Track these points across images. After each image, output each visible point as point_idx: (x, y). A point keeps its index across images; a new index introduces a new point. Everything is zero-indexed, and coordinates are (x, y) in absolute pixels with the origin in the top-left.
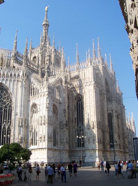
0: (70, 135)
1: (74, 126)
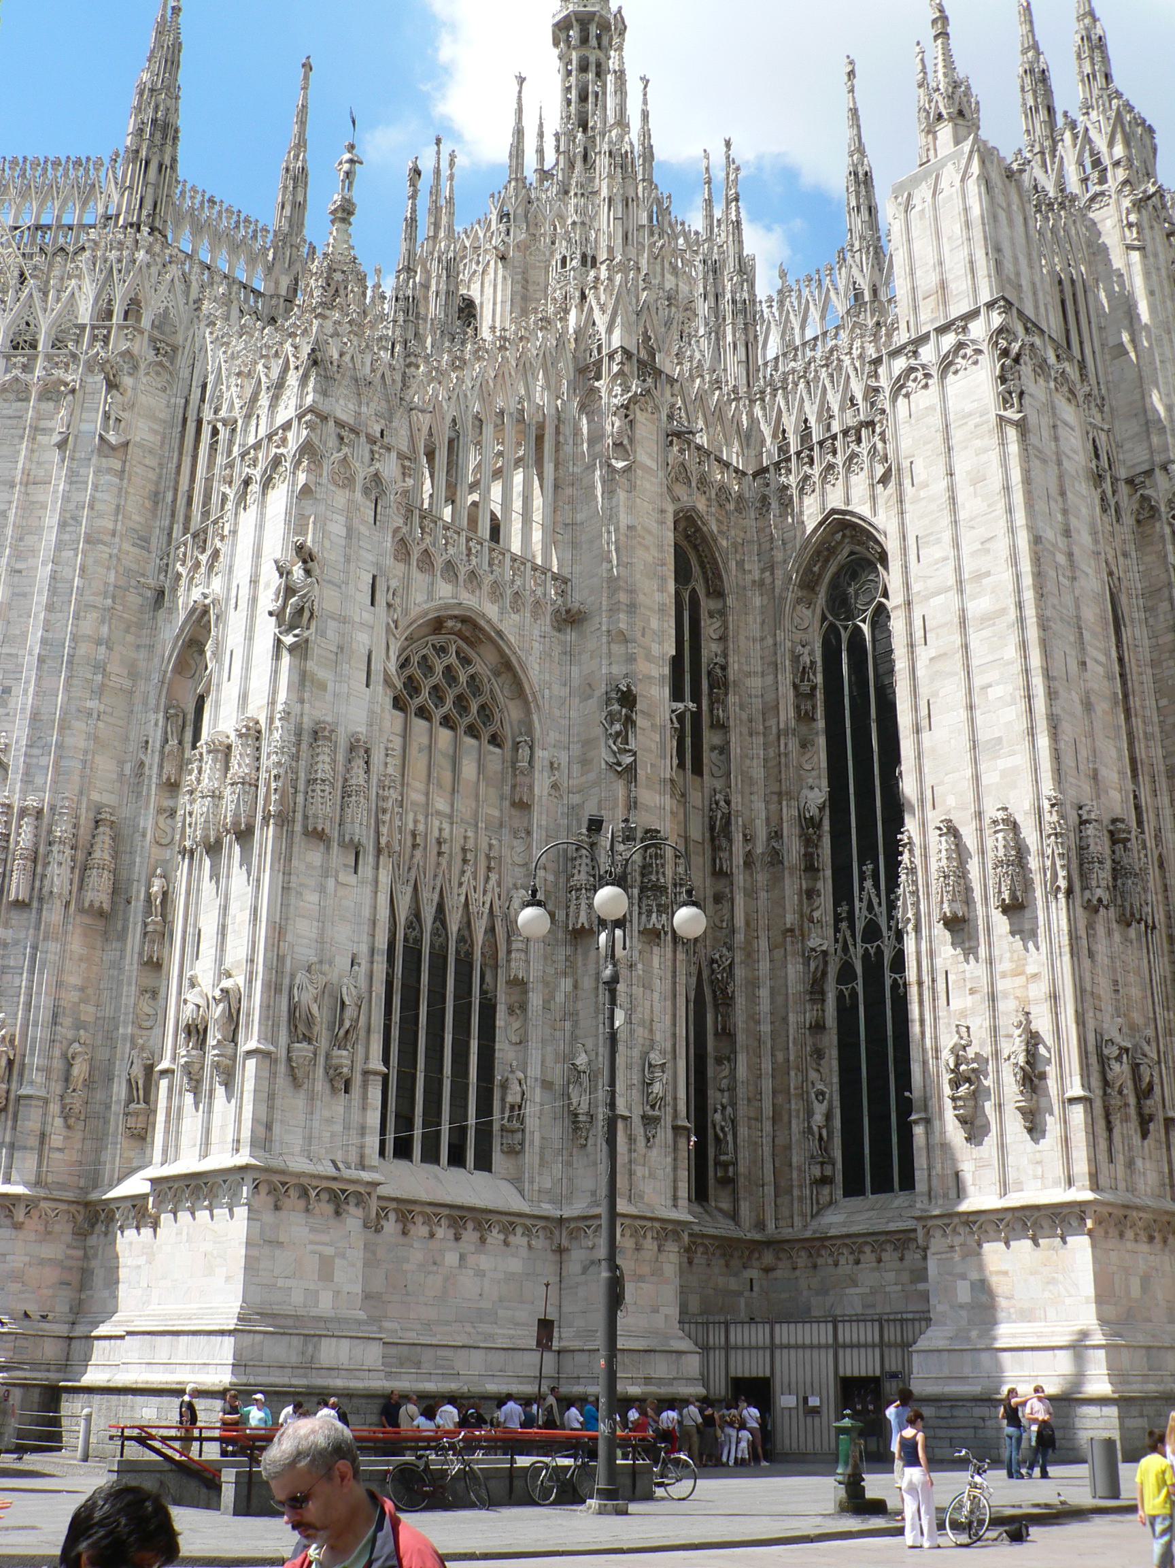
0: (741, 1038)
1: (790, 919)
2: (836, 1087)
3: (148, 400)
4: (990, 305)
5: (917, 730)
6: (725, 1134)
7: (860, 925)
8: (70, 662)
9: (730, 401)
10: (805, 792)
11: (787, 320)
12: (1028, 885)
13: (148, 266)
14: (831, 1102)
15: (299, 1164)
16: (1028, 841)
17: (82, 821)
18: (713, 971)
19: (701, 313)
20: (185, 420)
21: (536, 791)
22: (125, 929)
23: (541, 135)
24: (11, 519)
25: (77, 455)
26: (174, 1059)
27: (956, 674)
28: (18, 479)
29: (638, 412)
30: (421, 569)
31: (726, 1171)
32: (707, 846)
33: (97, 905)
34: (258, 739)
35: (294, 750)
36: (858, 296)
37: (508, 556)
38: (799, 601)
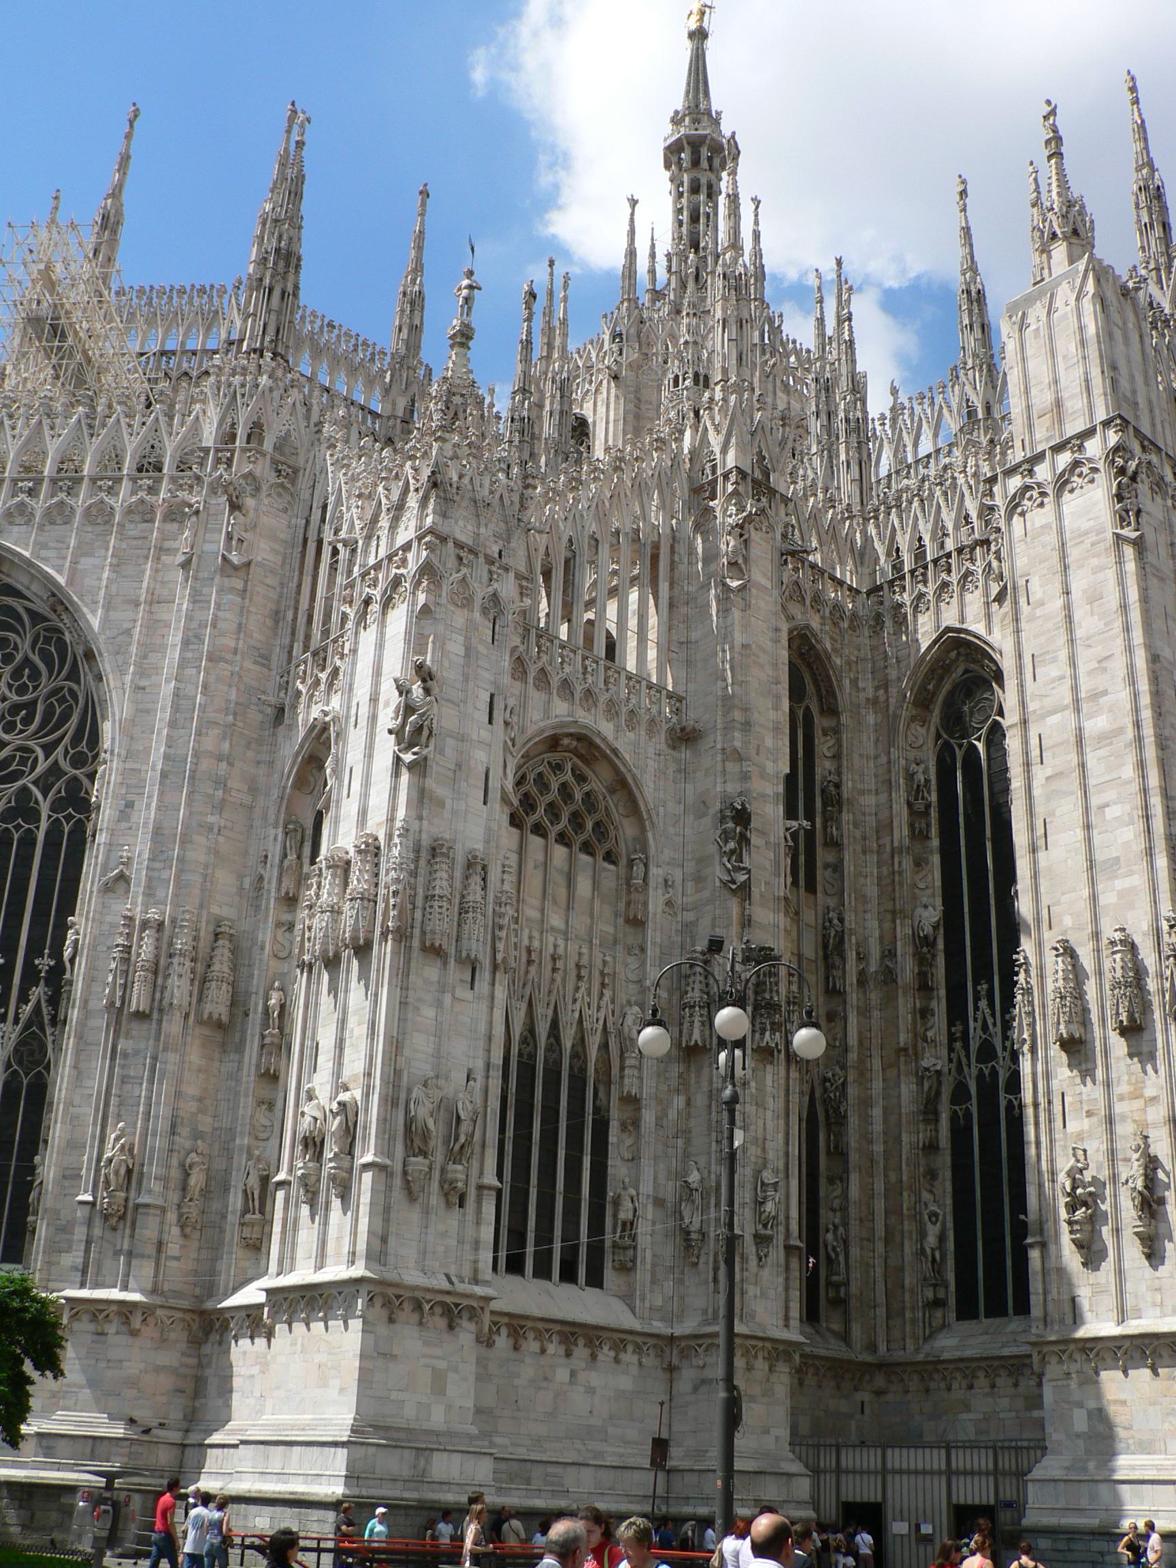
0: (854, 1157)
1: (904, 1038)
2: (949, 1209)
3: (270, 520)
4: (1106, 424)
5: (1034, 850)
6: (837, 1255)
7: (974, 1046)
8: (192, 778)
9: (844, 520)
10: (919, 910)
11: (900, 437)
12: (1146, 1007)
13: (271, 390)
14: (944, 1223)
15: (413, 1277)
16: (1147, 962)
17: (202, 934)
18: (825, 1090)
19: (812, 430)
20: (305, 540)
21: (651, 908)
22: (242, 1041)
23: (653, 255)
24: (136, 637)
25: (200, 575)
26: (290, 1171)
27: (1072, 793)
28: (142, 599)
29: (753, 532)
30: (537, 687)
31: (838, 1292)
32: (820, 963)
33: (216, 1016)
34: (376, 855)
35: (412, 867)
36: (971, 414)
37: (623, 674)
38: (913, 719)
